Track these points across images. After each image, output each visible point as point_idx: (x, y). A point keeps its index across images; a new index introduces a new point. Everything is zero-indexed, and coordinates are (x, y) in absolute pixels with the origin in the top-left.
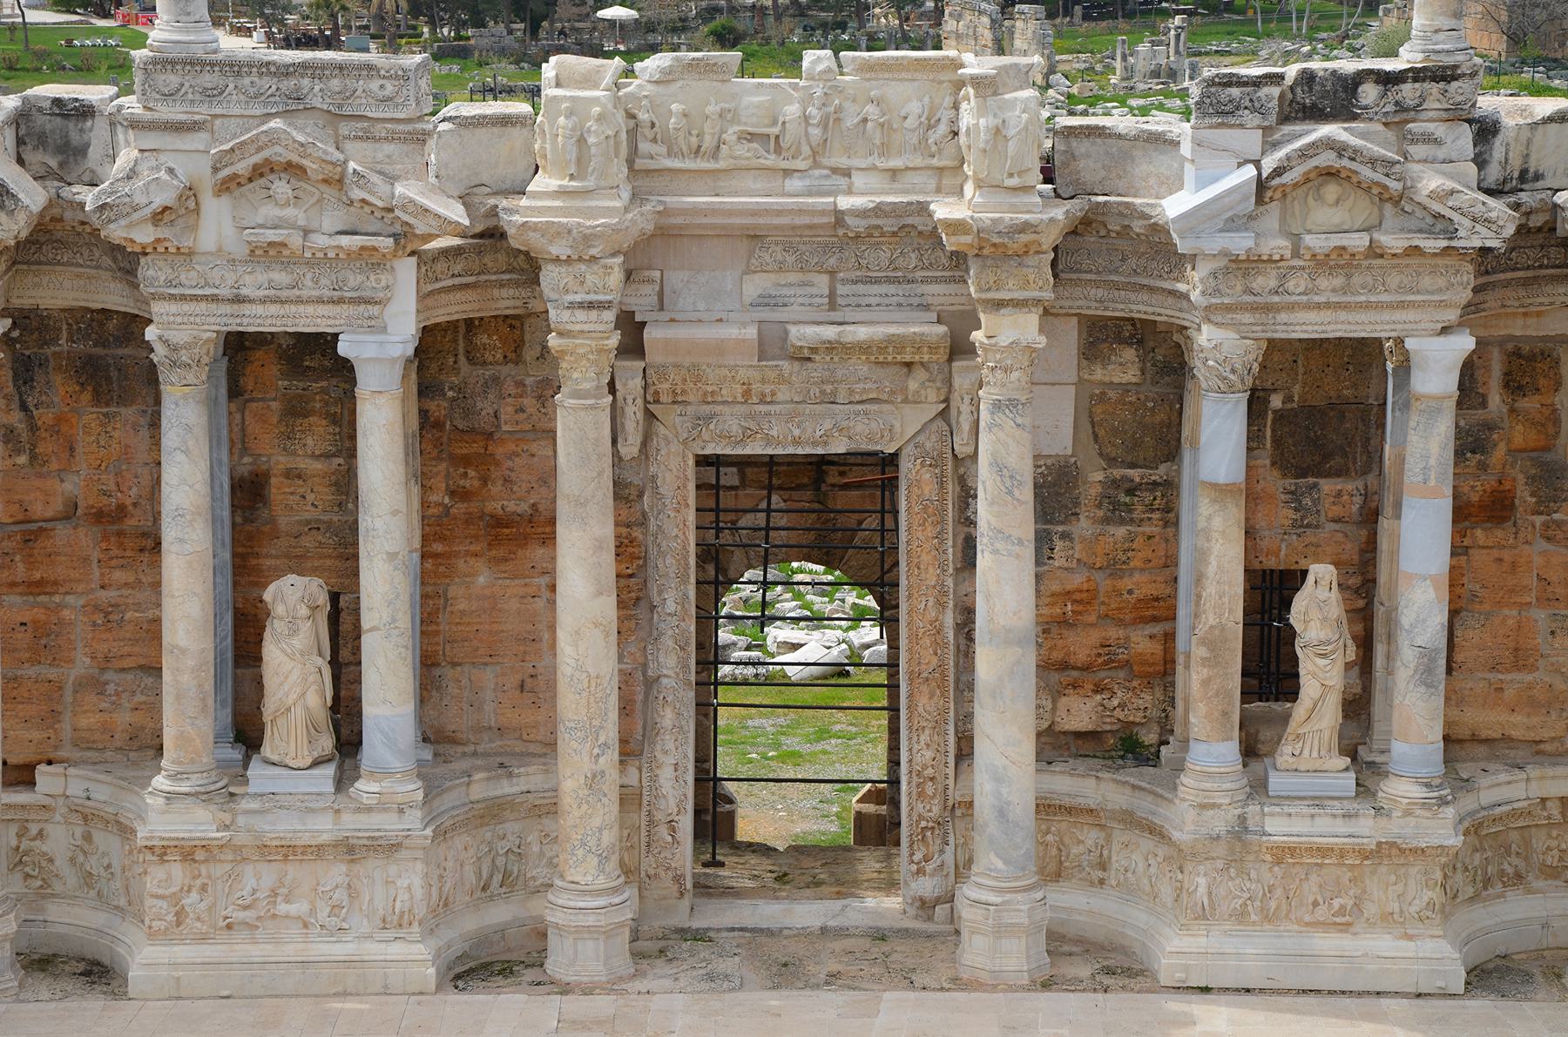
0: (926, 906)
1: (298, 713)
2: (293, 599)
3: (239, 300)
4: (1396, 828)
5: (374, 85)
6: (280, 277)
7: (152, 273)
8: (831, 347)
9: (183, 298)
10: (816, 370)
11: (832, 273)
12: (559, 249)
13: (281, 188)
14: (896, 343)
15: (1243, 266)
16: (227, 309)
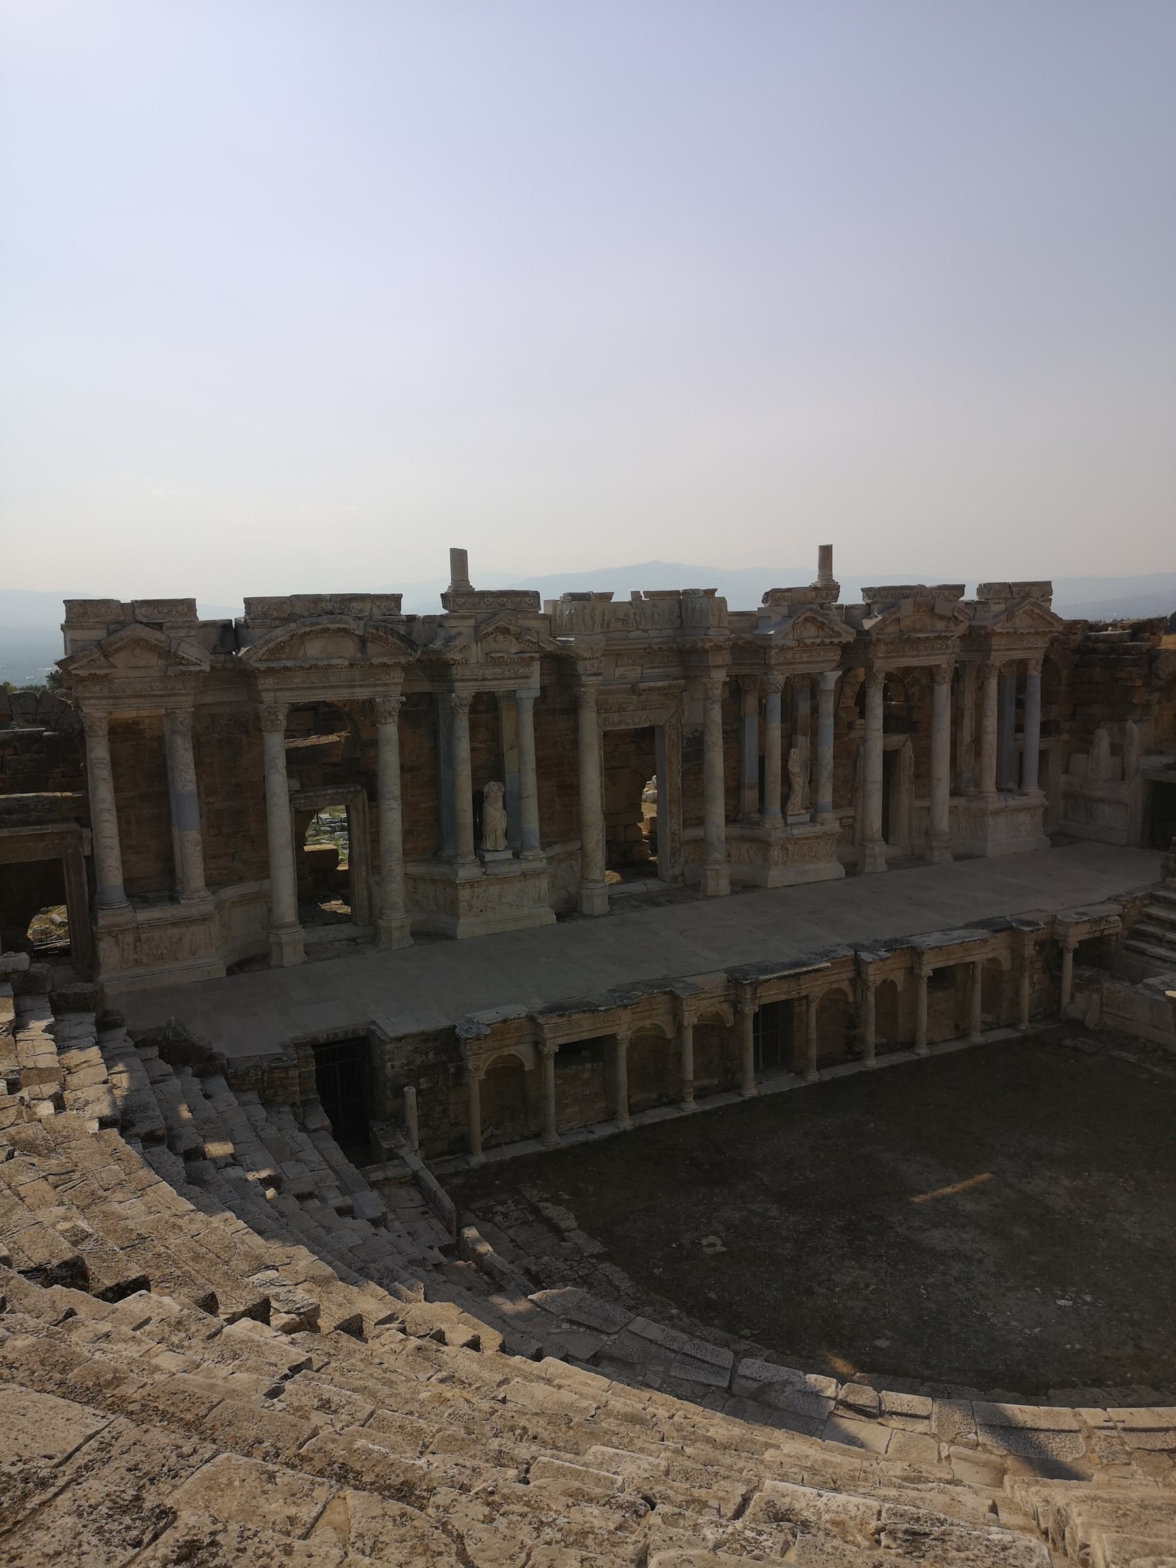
0: (675, 879)
1: (500, 833)
2: (493, 789)
3: (484, 680)
4: (827, 828)
5: (527, 599)
6: (497, 670)
7: (457, 672)
8: (650, 689)
9: (466, 680)
10: (642, 698)
11: (642, 666)
12: (587, 655)
13: (500, 637)
14: (670, 687)
15: (783, 649)
16: (479, 683)
